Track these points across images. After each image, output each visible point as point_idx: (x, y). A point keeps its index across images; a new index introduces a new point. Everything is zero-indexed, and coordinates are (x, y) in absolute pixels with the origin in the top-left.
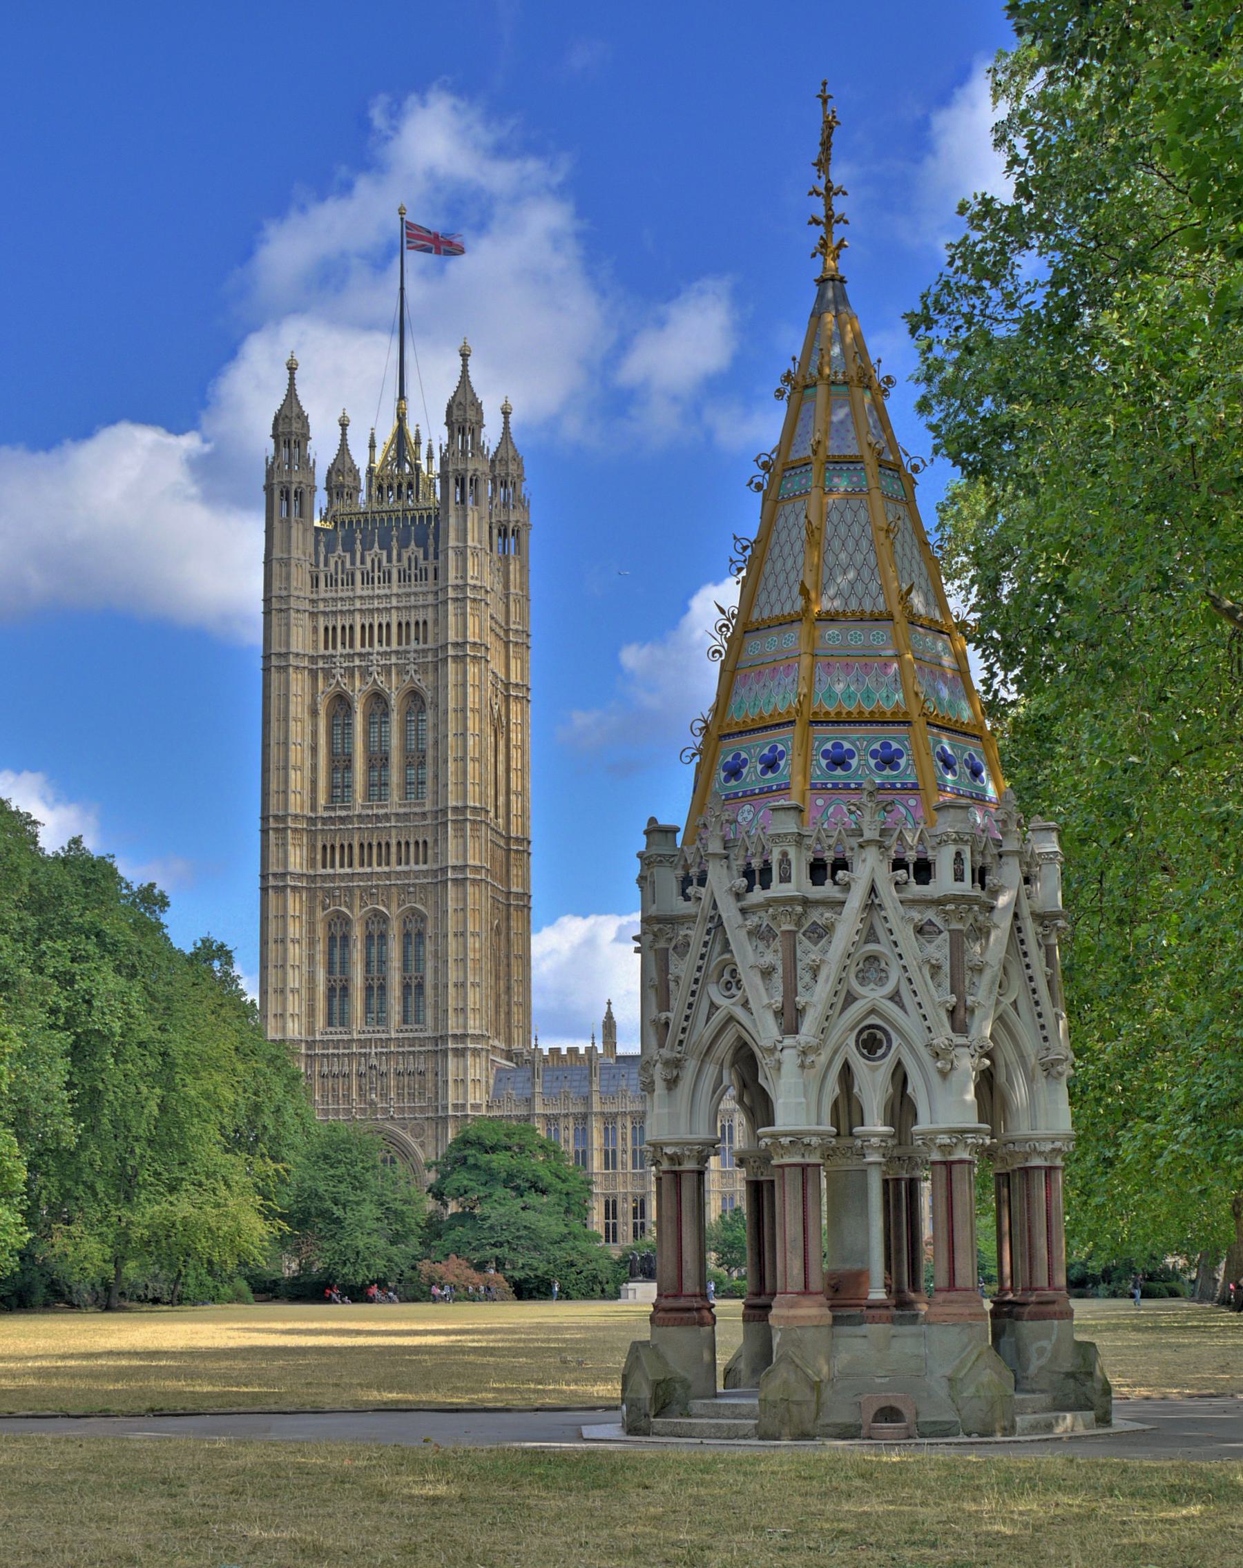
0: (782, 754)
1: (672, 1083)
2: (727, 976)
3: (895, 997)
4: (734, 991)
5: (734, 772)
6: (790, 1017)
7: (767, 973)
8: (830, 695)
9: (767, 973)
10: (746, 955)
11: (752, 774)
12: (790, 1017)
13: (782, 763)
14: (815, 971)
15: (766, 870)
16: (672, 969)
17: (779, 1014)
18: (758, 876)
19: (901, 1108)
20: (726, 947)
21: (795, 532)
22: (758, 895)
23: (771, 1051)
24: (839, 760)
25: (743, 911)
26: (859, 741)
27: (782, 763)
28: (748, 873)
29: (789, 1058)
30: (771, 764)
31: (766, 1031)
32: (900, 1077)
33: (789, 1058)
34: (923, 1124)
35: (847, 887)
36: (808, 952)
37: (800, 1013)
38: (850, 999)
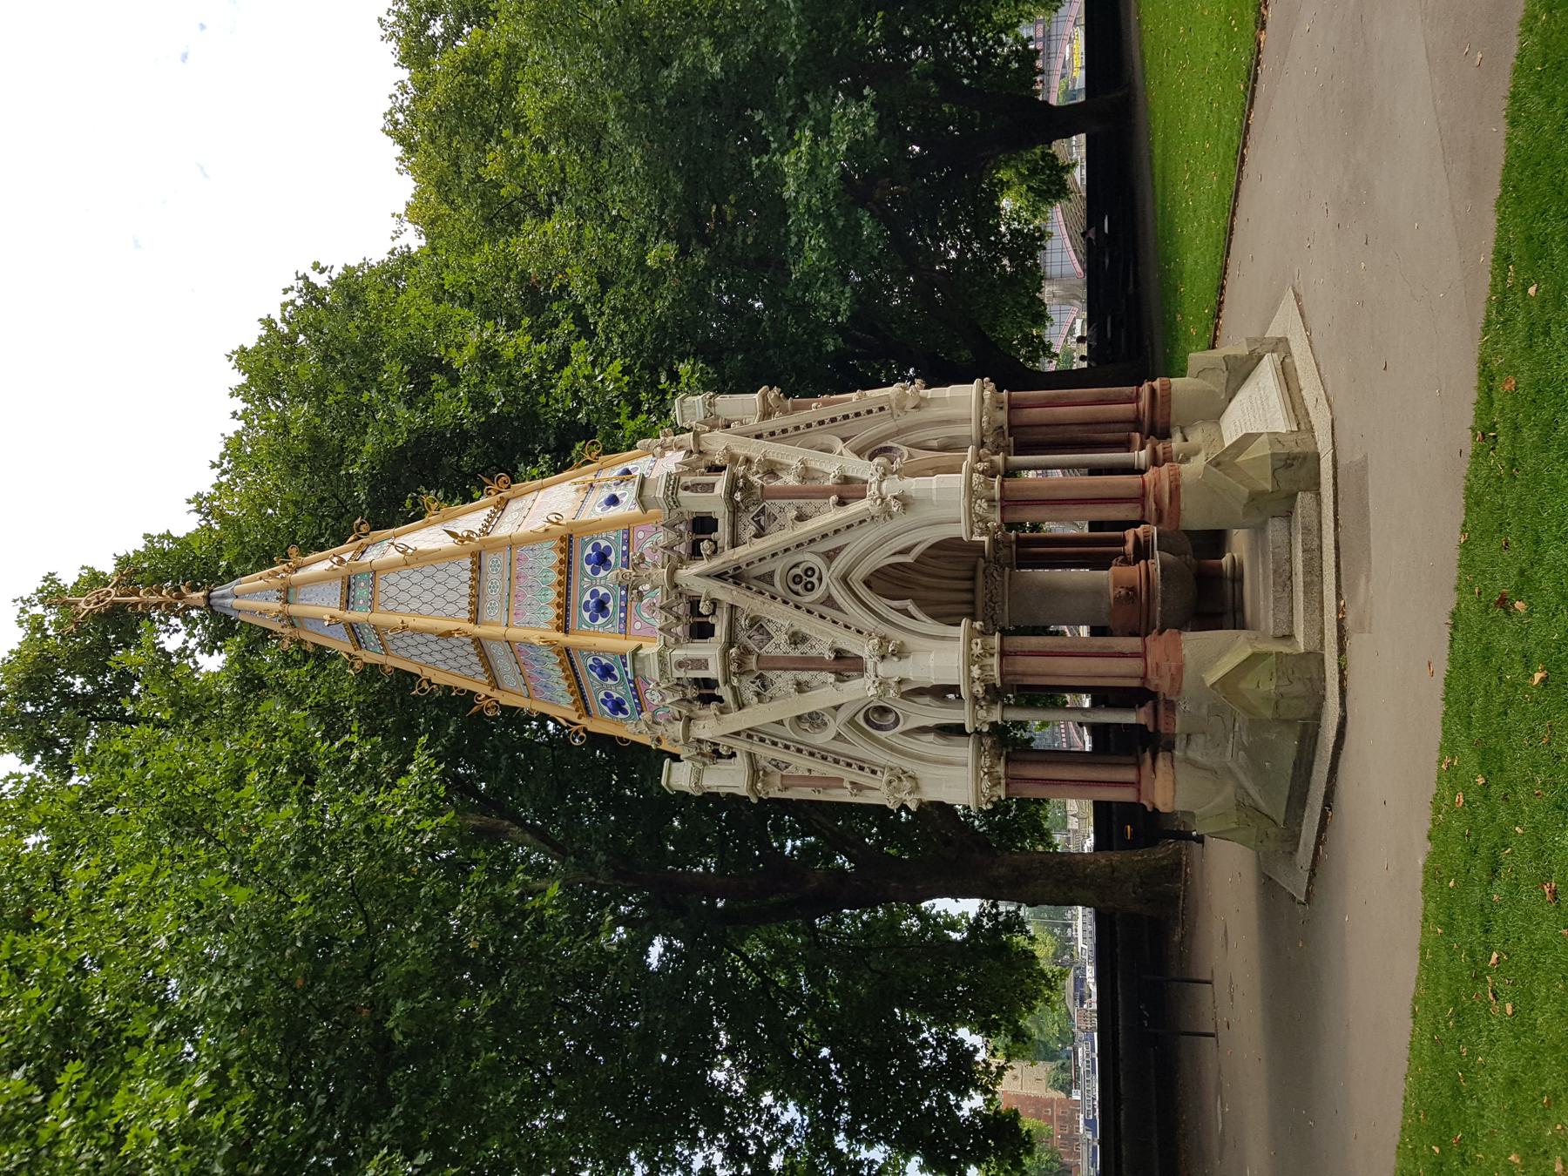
0: (596, 546)
1: (900, 653)
2: (799, 588)
3: (844, 440)
4: (814, 580)
7: (801, 518)
12: (848, 489)
13: (603, 544)
14: (806, 474)
16: (778, 653)
17: (842, 502)
20: (768, 578)
21: (404, 584)
22: (723, 533)
25: (734, 544)
27: (603, 544)
28: (695, 553)
29: (893, 486)
33: (893, 486)
35: (733, 459)
37: (846, 480)
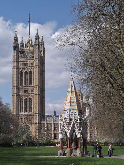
5: (65, 113)
6: (68, 130)
8: (71, 108)
9: (67, 127)
10: (65, 125)
11: (66, 113)
15: (67, 120)
17: (68, 130)
18: (66, 120)
19: (76, 136)
23: (67, 132)
24: (72, 113)
26: (73, 111)
30: (67, 113)
31: (67, 131)
32: (76, 133)
33: (68, 133)
34: (77, 137)
36: (70, 126)
38: (72, 129)
